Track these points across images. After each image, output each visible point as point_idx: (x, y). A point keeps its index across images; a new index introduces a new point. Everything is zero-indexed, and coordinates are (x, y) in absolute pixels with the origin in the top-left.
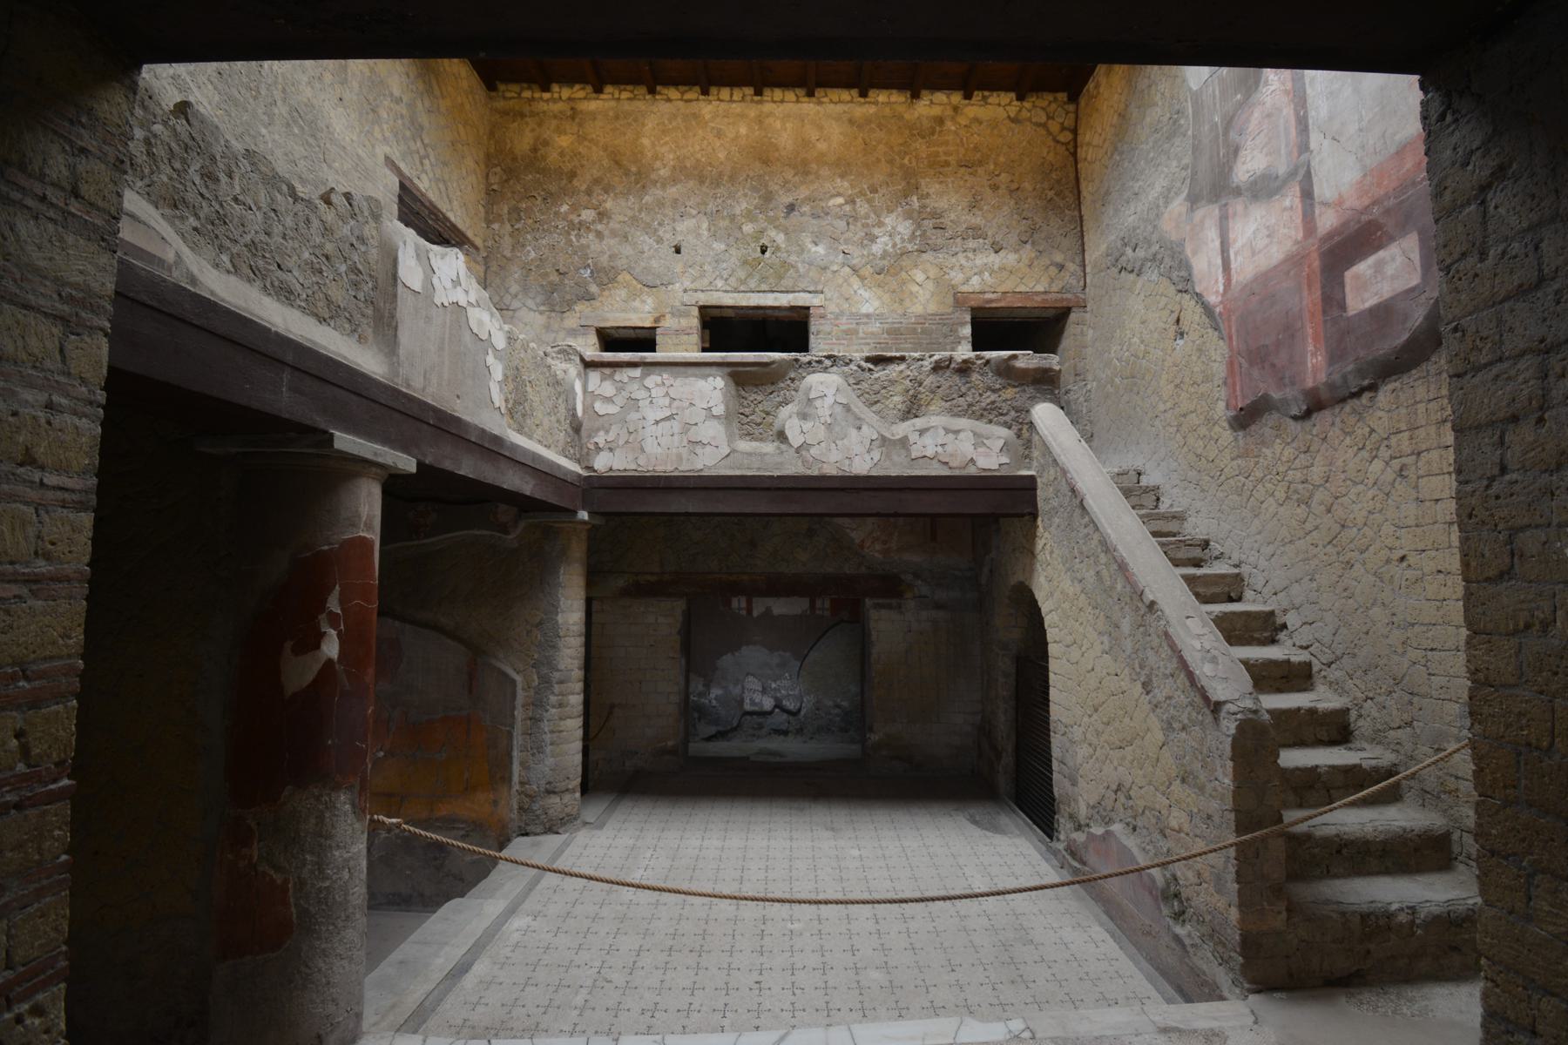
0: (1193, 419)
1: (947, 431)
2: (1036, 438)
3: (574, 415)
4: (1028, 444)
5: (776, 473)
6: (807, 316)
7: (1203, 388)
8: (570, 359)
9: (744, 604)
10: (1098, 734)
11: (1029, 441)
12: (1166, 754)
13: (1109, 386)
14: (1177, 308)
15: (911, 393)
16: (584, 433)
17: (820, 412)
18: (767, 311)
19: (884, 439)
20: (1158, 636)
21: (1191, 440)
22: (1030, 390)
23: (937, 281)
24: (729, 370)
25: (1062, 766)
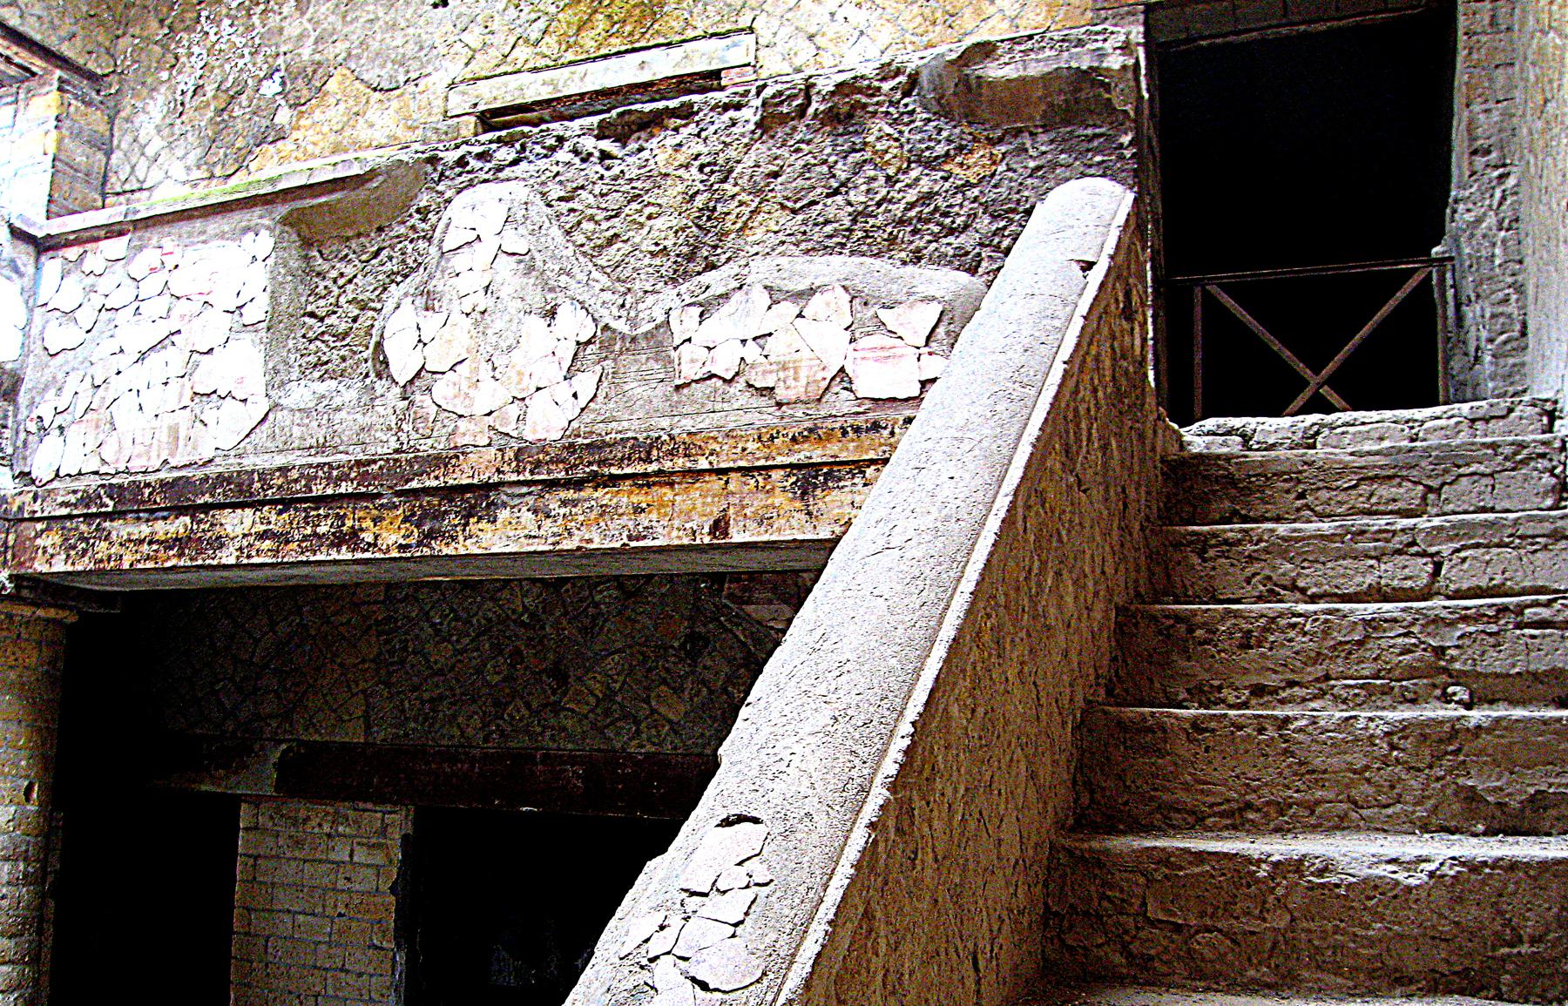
15: (700, 201)
24: (282, 210)
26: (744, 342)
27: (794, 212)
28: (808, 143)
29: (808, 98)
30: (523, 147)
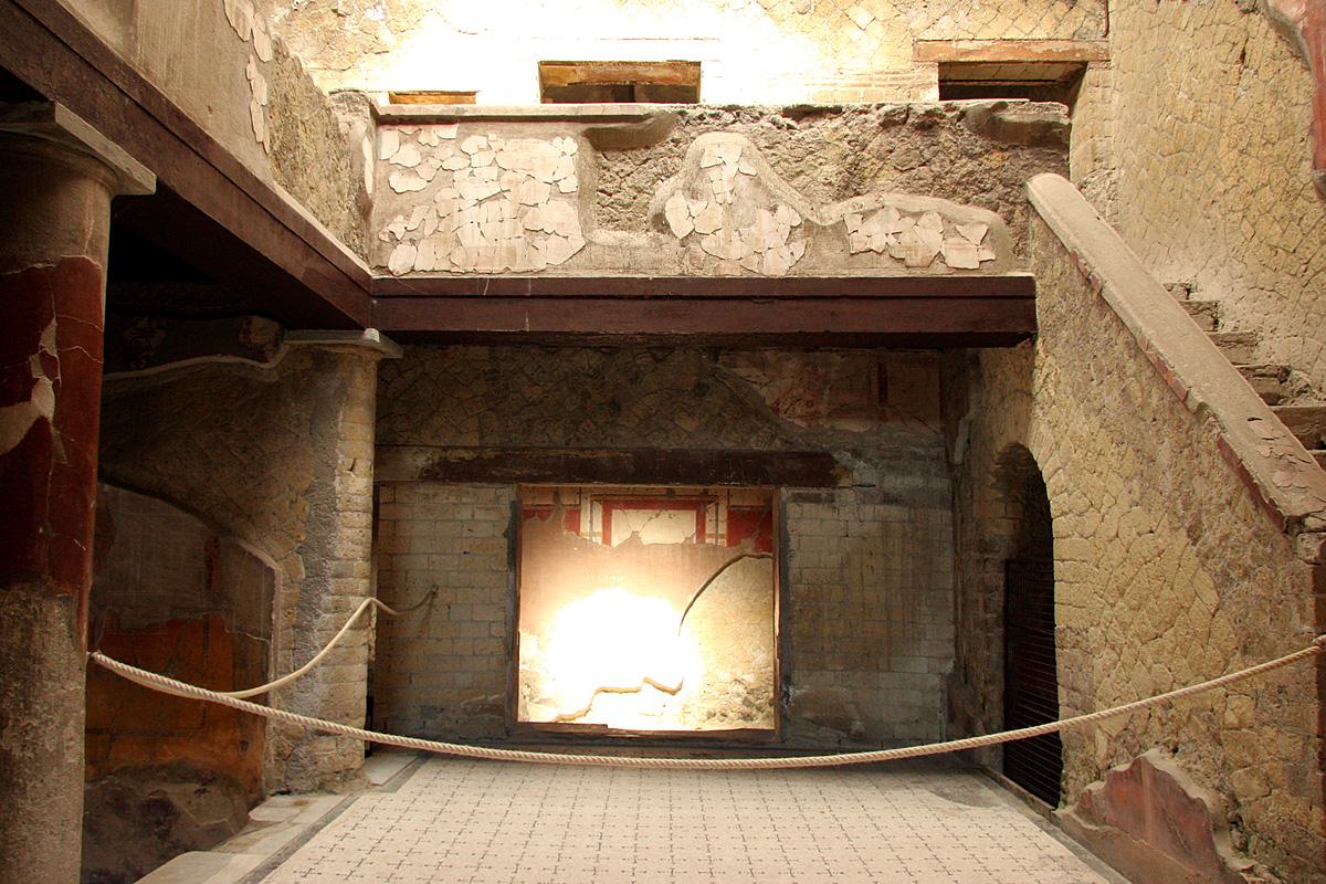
0: (1267, 195)
1: (903, 213)
2: (1034, 222)
3: (362, 189)
4: (1023, 235)
5: (652, 275)
6: (698, 79)
7: (1279, 149)
8: (356, 110)
9: (598, 528)
10: (1124, 626)
11: (1024, 229)
12: (1222, 623)
13: (1143, 170)
14: (1241, 39)
15: (849, 159)
16: (374, 217)
17: (716, 186)
18: (641, 70)
19: (808, 228)
20: (1210, 453)
21: (1263, 227)
22: (1026, 155)
23: (887, 23)
25: (1072, 693)
26: (887, 235)
27: (901, 171)
28: (909, 137)
29: (908, 115)
30: (738, 115)
